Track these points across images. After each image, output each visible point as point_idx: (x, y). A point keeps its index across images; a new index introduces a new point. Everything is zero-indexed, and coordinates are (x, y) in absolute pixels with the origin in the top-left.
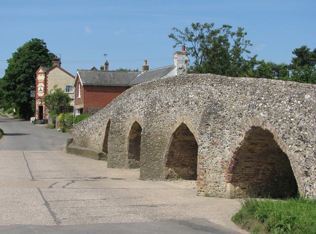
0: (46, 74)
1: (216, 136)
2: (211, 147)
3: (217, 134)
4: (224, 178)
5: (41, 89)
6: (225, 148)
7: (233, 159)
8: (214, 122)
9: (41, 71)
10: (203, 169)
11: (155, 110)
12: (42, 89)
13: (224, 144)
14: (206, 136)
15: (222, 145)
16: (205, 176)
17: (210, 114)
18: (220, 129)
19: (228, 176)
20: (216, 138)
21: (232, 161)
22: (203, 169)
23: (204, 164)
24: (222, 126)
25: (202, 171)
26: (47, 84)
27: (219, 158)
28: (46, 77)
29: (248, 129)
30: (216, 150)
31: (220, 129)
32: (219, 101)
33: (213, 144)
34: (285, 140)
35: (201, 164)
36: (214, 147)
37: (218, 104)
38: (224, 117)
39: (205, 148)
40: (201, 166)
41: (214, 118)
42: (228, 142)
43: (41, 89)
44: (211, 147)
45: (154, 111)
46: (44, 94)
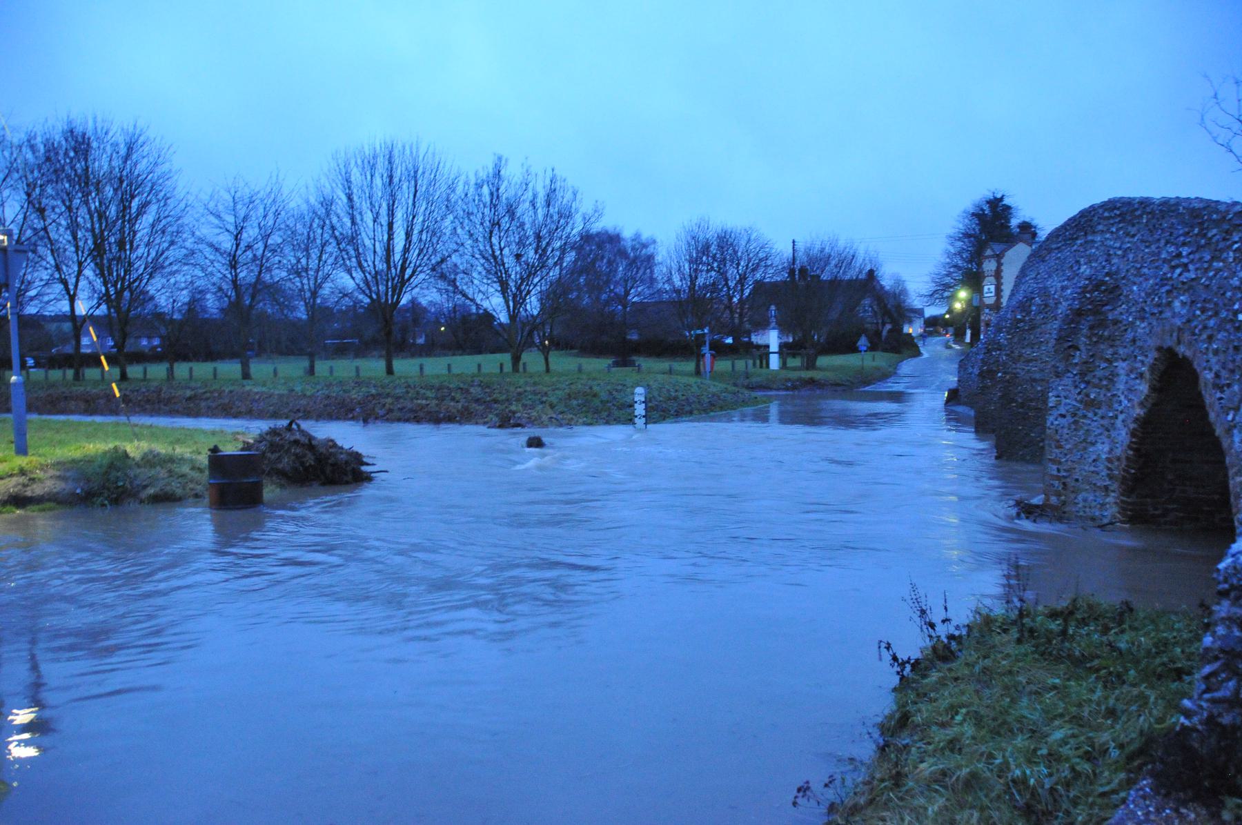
0: (999, 257)
1: (1095, 381)
2: (1080, 413)
3: (1099, 373)
4: (1115, 509)
5: (989, 289)
6: (1116, 417)
7: (1131, 452)
8: (1089, 338)
9: (989, 252)
10: (1058, 478)
11: (1029, 313)
12: (992, 288)
13: (1116, 405)
14: (1067, 381)
15: (1110, 407)
16: (1063, 498)
17: (1079, 313)
18: (1107, 360)
19: (1122, 501)
20: (1096, 386)
21: (1128, 458)
22: (1058, 478)
23: (1060, 463)
24: (1110, 351)
25: (1056, 483)
26: (1002, 278)
27: (1102, 449)
28: (1000, 265)
29: (1153, 355)
30: (1093, 423)
31: (1107, 360)
32: (1107, 274)
33: (1091, 404)
34: (1219, 395)
35: (1053, 461)
36: (1090, 415)
37: (1104, 283)
38: (1116, 322)
39: (1063, 416)
40: (1055, 467)
41: (1091, 328)
42: (1122, 398)
43: (989, 289)
44: (1080, 413)
45: (1027, 318)
46: (995, 298)
